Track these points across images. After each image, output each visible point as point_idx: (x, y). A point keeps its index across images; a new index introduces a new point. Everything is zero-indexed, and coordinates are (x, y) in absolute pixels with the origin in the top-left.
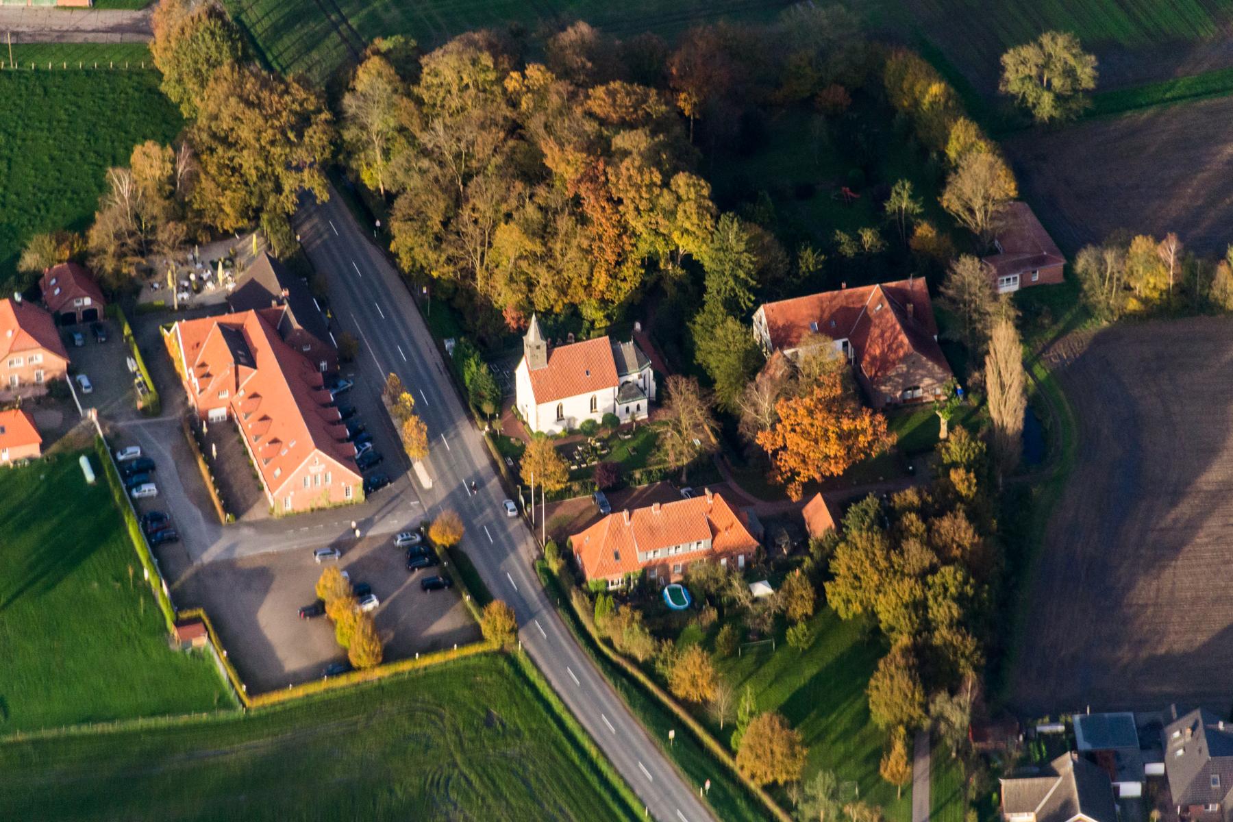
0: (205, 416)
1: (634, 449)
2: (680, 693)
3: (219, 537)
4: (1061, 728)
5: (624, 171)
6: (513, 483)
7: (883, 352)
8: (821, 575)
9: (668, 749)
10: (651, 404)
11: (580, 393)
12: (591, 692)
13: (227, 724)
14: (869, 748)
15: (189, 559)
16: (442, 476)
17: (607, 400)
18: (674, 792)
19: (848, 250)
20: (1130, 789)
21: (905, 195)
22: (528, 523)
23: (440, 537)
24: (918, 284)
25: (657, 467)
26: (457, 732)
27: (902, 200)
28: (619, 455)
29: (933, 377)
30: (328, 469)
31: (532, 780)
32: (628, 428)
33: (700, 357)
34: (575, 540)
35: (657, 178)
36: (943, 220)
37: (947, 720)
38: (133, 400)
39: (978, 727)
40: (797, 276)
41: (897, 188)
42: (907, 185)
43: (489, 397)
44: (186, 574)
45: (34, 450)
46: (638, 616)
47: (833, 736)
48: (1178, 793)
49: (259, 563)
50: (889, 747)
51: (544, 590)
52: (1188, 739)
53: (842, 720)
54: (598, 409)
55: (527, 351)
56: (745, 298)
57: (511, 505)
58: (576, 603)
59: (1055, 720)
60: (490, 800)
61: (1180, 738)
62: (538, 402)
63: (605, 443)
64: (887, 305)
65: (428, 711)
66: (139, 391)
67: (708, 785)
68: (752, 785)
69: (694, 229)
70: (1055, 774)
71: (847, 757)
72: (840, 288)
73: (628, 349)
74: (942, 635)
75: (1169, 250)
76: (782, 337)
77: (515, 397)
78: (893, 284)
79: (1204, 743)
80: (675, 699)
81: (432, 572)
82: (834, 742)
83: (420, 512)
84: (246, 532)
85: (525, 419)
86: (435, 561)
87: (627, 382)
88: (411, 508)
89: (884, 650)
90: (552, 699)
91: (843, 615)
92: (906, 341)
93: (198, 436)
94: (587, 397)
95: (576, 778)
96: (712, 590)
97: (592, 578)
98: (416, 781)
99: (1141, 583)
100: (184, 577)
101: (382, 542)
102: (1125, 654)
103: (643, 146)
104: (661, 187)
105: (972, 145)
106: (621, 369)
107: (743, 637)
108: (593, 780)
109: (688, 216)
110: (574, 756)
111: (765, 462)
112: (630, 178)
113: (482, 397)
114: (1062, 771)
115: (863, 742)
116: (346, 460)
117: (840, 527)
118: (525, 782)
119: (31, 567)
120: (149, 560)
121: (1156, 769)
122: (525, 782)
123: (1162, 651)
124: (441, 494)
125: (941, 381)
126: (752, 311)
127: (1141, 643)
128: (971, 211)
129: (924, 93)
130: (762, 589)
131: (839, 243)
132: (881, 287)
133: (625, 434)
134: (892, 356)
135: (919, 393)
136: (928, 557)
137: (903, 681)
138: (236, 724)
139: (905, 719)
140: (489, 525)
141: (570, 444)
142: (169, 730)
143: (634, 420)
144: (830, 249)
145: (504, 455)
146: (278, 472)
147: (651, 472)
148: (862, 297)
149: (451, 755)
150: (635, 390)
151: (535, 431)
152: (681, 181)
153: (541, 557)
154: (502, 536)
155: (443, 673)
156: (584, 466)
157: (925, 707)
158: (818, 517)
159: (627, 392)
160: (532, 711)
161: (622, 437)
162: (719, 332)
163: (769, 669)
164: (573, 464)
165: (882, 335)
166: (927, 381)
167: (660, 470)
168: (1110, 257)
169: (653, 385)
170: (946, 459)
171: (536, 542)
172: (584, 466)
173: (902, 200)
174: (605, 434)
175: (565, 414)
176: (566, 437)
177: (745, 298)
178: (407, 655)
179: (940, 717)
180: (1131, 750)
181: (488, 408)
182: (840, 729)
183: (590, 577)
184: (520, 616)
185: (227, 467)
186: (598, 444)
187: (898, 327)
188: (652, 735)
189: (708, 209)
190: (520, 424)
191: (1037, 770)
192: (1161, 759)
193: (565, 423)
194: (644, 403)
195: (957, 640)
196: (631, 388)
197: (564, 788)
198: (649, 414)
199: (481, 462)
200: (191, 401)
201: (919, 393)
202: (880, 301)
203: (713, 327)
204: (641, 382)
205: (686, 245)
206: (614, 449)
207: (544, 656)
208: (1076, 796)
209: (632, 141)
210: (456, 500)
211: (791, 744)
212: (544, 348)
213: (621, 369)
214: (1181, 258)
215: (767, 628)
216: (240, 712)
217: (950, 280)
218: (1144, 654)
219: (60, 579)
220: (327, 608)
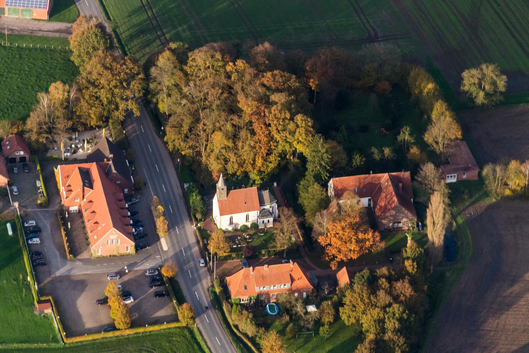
1: (264, 240)
3: (66, 265)
5: (273, 111)
6: (204, 251)
10: (275, 220)
11: (241, 212)
15: (50, 273)
17: (254, 216)
19: (377, 157)
21: (407, 133)
25: (273, 249)
27: (405, 135)
28: (256, 242)
29: (407, 218)
30: (118, 237)
32: (263, 230)
33: (300, 201)
35: (288, 116)
40: (351, 167)
41: (404, 129)
42: (408, 129)
43: (200, 211)
49: (82, 278)
54: (250, 220)
55: (218, 190)
56: (325, 175)
57: (202, 261)
62: (221, 215)
63: (251, 236)
69: (302, 141)
72: (369, 173)
73: (266, 194)
77: (212, 212)
83: (160, 261)
84: (78, 263)
85: (216, 222)
87: (264, 209)
88: (156, 259)
94: (245, 214)
100: (46, 282)
103: (283, 100)
104: (289, 120)
106: (262, 202)
109: (301, 134)
112: (275, 115)
113: (196, 210)
116: (128, 234)
120: (31, 272)
124: (171, 253)
125: (411, 220)
131: (373, 153)
132: (389, 175)
133: (261, 233)
135: (401, 225)
140: (191, 269)
141: (235, 236)
143: (265, 227)
144: (369, 156)
145: (203, 238)
146: (95, 237)
147: (270, 251)
148: (380, 178)
150: (268, 213)
151: (219, 228)
152: (299, 118)
156: (239, 246)
159: (264, 214)
161: (259, 234)
162: (310, 190)
164: (234, 245)
165: (386, 197)
166: (405, 220)
167: (274, 251)
172: (239, 246)
174: (252, 232)
175: (234, 222)
176: (233, 232)
177: (325, 175)
181: (199, 216)
186: (248, 237)
187: (394, 193)
189: (310, 132)
190: (213, 225)
193: (233, 225)
194: (271, 219)
196: (266, 212)
198: (274, 225)
199: (192, 240)
201: (401, 225)
203: (308, 187)
204: (271, 210)
205: (300, 148)
206: (255, 240)
209: (278, 98)
212: (225, 190)
213: (262, 202)
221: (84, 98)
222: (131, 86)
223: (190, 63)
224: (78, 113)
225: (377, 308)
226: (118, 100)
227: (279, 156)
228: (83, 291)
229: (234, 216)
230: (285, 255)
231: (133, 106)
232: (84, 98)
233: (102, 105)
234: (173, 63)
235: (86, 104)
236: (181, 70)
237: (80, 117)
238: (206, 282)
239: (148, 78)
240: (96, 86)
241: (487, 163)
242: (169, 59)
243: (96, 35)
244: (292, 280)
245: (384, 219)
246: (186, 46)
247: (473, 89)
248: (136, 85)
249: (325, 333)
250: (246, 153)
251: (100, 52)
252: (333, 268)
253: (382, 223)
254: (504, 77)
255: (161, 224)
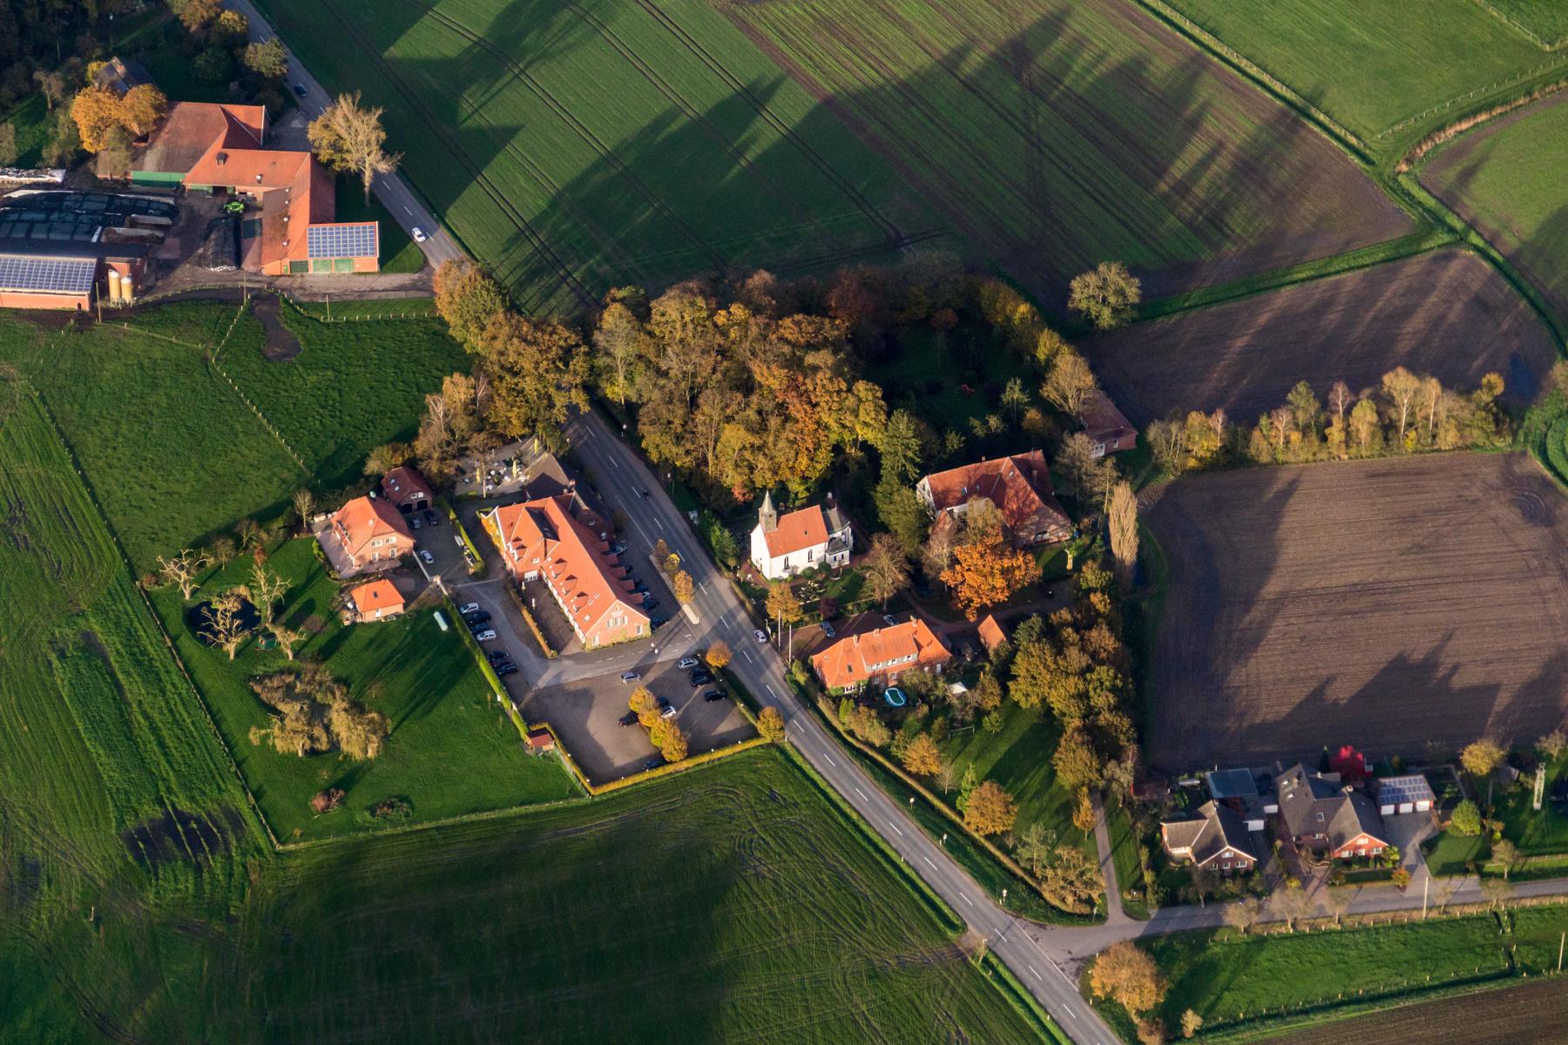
0: (522, 579)
2: (913, 769)
4: (1197, 782)
7: (1018, 508)
8: (1004, 675)
9: (909, 811)
12: (844, 771)
13: (578, 808)
14: (1056, 804)
16: (705, 614)
18: (920, 844)
19: (980, 431)
20: (1256, 825)
21: (1017, 388)
22: (775, 646)
24: (1037, 455)
26: (751, 807)
27: (1014, 393)
28: (833, 592)
31: (813, 840)
32: (836, 572)
33: (882, 516)
34: (816, 659)
36: (1047, 407)
37: (1118, 781)
38: (465, 567)
39: (1138, 786)
41: (1009, 384)
42: (1018, 382)
44: (529, 696)
45: (399, 609)
46: (873, 713)
47: (1029, 796)
48: (1294, 826)
50: (1078, 804)
51: (796, 696)
52: (1296, 786)
53: (1034, 781)
56: (912, 471)
58: (822, 705)
59: (1191, 777)
60: (785, 856)
61: (1289, 785)
63: (821, 583)
64: (1017, 472)
65: (727, 792)
66: (469, 560)
67: (945, 837)
68: (976, 835)
70: (1202, 817)
71: (1042, 811)
73: (833, 513)
74: (1105, 718)
75: (1218, 421)
76: (942, 500)
78: (1019, 456)
79: (1309, 789)
80: (909, 774)
81: (711, 687)
82: (1030, 801)
83: (694, 642)
86: (711, 678)
89: (1061, 731)
90: (817, 778)
91: (1023, 705)
92: (1037, 498)
93: (519, 592)
94: (806, 550)
95: (845, 836)
96: (923, 691)
97: (831, 685)
98: (727, 844)
99: (1233, 672)
101: (669, 666)
102: (1232, 724)
105: (1058, 349)
106: (830, 529)
107: (952, 724)
108: (858, 836)
110: (841, 819)
111: (949, 593)
114: (1207, 815)
115: (1051, 799)
117: (1011, 640)
118: (808, 840)
119: (413, 696)
121: (1272, 809)
122: (808, 840)
123: (1258, 721)
124: (707, 628)
126: (917, 481)
127: (1242, 715)
128: (1066, 399)
129: (1014, 310)
130: (958, 688)
131: (973, 427)
134: (1027, 510)
136: (1085, 660)
137: (1083, 754)
138: (585, 807)
139: (1087, 781)
140: (746, 649)
142: (536, 815)
144: (966, 431)
148: (998, 466)
149: (750, 824)
153: (790, 672)
154: (757, 658)
155: (732, 763)
157: (1100, 771)
158: (992, 632)
159: (834, 545)
160: (805, 788)
162: (896, 498)
163: (973, 748)
165: (1017, 493)
168: (1174, 428)
169: (851, 539)
170: (1084, 586)
171: (783, 661)
173: (1014, 393)
174: (820, 578)
177: (912, 471)
178: (706, 751)
179: (1111, 780)
180: (1252, 796)
182: (1033, 791)
183: (829, 685)
184: (785, 716)
185: (544, 615)
188: (895, 801)
191: (1184, 814)
192: (1276, 802)
194: (847, 553)
195: (1116, 720)
197: (838, 844)
199: (732, 602)
200: (510, 565)
202: (1011, 469)
203: (891, 494)
207: (805, 745)
208: (1222, 833)
210: (718, 631)
211: (1007, 804)
214: (1225, 427)
215: (969, 718)
216: (587, 799)
217: (1064, 451)
218: (1245, 724)
219: (435, 705)
220: (640, 718)
221: (499, 395)
222: (571, 367)
223: (656, 317)
224: (492, 420)
225: (1071, 677)
226: (552, 390)
227: (832, 451)
229: (791, 555)
230: (885, 608)
231: (579, 398)
232: (499, 395)
233: (527, 402)
234: (629, 322)
235: (504, 404)
236: (641, 329)
237: (494, 425)
239: (593, 350)
240: (516, 374)
241: (1151, 420)
242: (621, 315)
243: (488, 290)
244: (919, 647)
245: (1022, 530)
246: (642, 292)
247: (1094, 309)
248: (579, 364)
249: (993, 725)
250: (782, 452)
251: (501, 316)
252: (972, 620)
253: (1019, 537)
254: (1137, 281)
255: (681, 585)
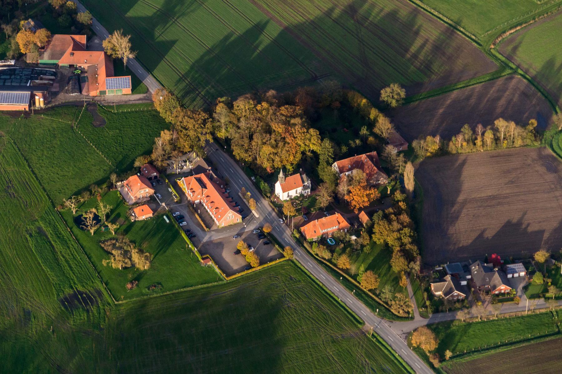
2: (341, 267)
6: (280, 214)
7: (369, 172)
9: (341, 282)
12: (316, 269)
13: (222, 285)
16: (261, 214)
21: (365, 129)
23: (266, 230)
24: (374, 153)
27: (364, 131)
28: (306, 204)
31: (307, 293)
34: (302, 229)
36: (376, 136)
37: (414, 269)
38: (173, 199)
40: (341, 153)
44: (200, 245)
45: (151, 215)
46: (325, 247)
47: (382, 275)
50: (401, 278)
57: (281, 220)
58: (305, 245)
60: (298, 300)
64: (368, 159)
67: (354, 291)
68: (365, 290)
71: (387, 280)
72: (355, 156)
74: (408, 247)
76: (342, 170)
78: (368, 154)
80: (339, 269)
81: (265, 240)
83: (257, 224)
86: (265, 237)
88: (254, 223)
89: (392, 252)
90: (306, 271)
92: (376, 169)
94: (295, 190)
95: (318, 292)
98: (277, 296)
105: (378, 115)
107: (353, 250)
108: (323, 292)
110: (316, 286)
111: (348, 204)
115: (390, 276)
118: (305, 294)
119: (159, 246)
122: (305, 294)
124: (262, 219)
129: (361, 101)
130: (354, 238)
134: (372, 173)
136: (399, 226)
137: (402, 260)
139: (403, 269)
148: (361, 157)
149: (284, 289)
153: (293, 233)
154: (281, 229)
155: (276, 266)
157: (408, 266)
158: (364, 217)
159: (305, 188)
160: (302, 275)
163: (361, 259)
165: (368, 167)
173: (364, 131)
174: (300, 199)
177: (331, 160)
178: (266, 263)
179: (412, 269)
182: (383, 273)
184: (293, 249)
185: (203, 216)
188: (335, 279)
194: (309, 190)
195: (412, 247)
197: (316, 295)
199: (270, 209)
200: (189, 198)
202: (366, 158)
207: (300, 259)
216: (225, 282)
219: (167, 249)
226: (199, 135)
227: (301, 154)
228: (223, 248)
232: (181, 137)
238: (288, 232)
241: (413, 140)
243: (174, 99)
244: (339, 223)
247: (390, 100)
248: (209, 125)
252: (356, 213)
